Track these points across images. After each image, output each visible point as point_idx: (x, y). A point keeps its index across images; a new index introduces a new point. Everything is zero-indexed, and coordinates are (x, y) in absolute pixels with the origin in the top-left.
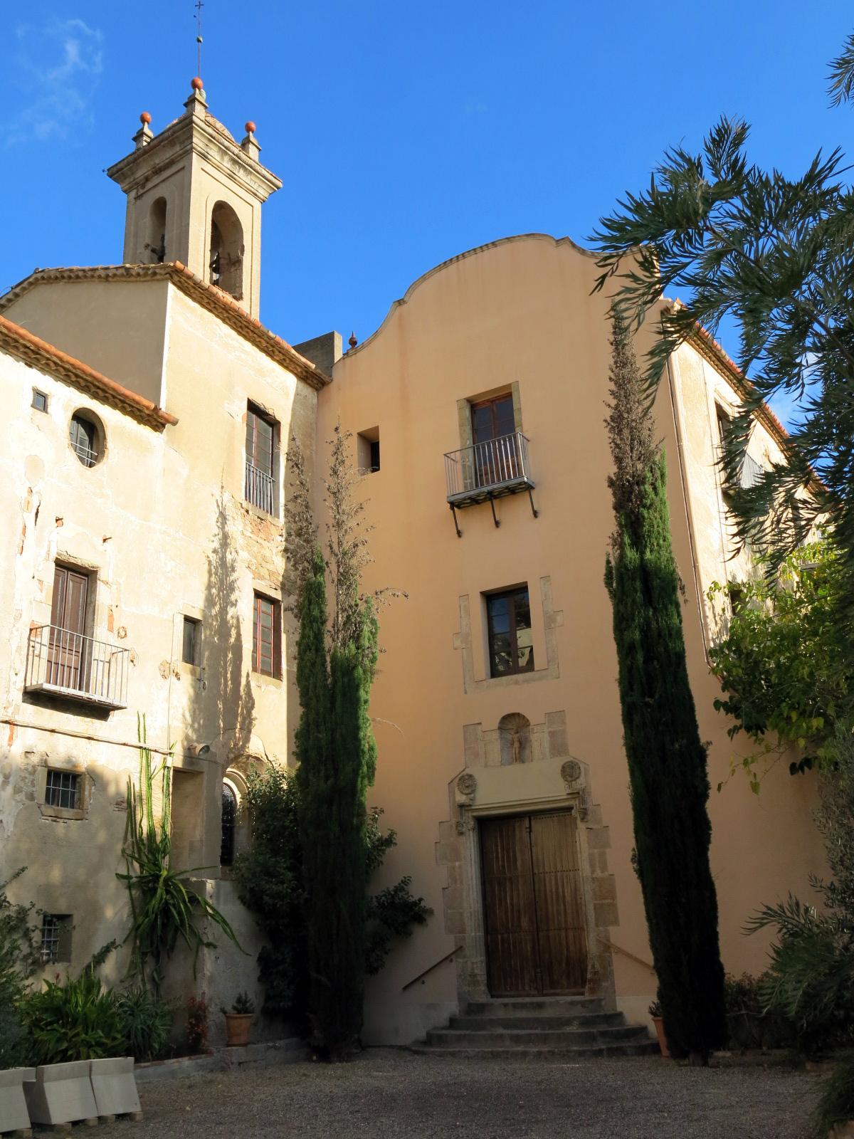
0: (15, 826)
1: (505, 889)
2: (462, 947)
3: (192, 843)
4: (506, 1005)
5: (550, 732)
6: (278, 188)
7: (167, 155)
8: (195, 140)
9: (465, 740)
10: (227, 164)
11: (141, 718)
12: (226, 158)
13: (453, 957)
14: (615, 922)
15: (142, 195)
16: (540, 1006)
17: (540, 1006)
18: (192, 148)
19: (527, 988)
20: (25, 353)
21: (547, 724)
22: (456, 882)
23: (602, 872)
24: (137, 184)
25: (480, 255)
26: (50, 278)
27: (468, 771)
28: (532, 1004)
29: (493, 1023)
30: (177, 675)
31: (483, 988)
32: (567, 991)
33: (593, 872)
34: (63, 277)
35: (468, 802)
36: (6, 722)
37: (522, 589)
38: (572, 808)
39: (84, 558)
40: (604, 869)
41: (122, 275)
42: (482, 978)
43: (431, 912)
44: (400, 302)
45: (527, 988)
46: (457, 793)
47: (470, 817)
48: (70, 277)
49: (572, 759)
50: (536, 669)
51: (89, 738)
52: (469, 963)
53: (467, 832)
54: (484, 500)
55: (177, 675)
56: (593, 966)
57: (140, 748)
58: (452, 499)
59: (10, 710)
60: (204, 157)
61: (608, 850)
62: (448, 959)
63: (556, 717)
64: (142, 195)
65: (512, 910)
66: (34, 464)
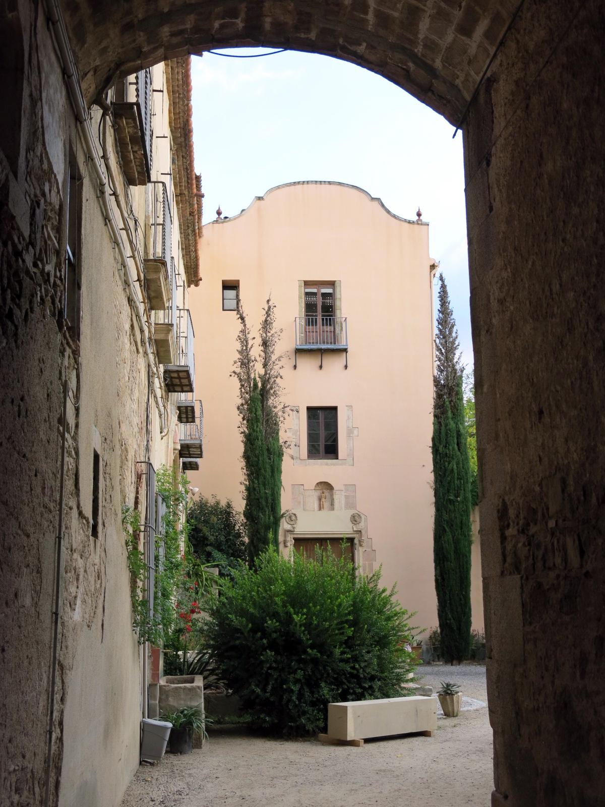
9: (293, 493)
25: (318, 185)
37: (335, 409)
44: (260, 198)
50: (339, 458)
61: (374, 563)
63: (351, 488)
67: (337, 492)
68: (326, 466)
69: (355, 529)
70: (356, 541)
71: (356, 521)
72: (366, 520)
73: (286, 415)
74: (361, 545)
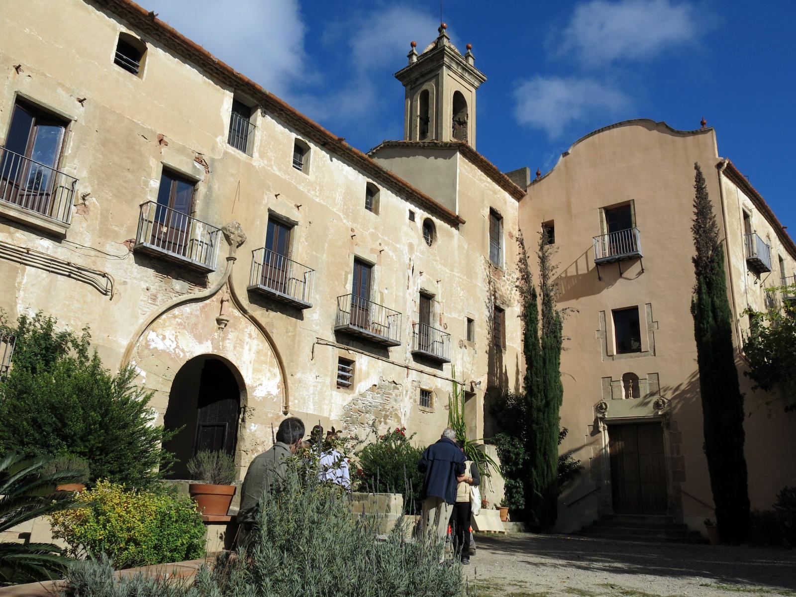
0: (410, 413)
3: (470, 427)
6: (484, 80)
7: (429, 67)
8: (445, 59)
10: (460, 70)
11: (453, 367)
12: (460, 67)
15: (414, 88)
18: (444, 63)
20: (407, 194)
24: (411, 81)
26: (392, 145)
30: (465, 346)
34: (399, 145)
36: (406, 367)
39: (430, 290)
41: (433, 146)
48: (403, 146)
51: (435, 376)
54: (614, 262)
55: (465, 346)
57: (453, 381)
58: (597, 261)
59: (407, 361)
60: (449, 67)
64: (414, 88)
66: (411, 246)
73: (565, 316)
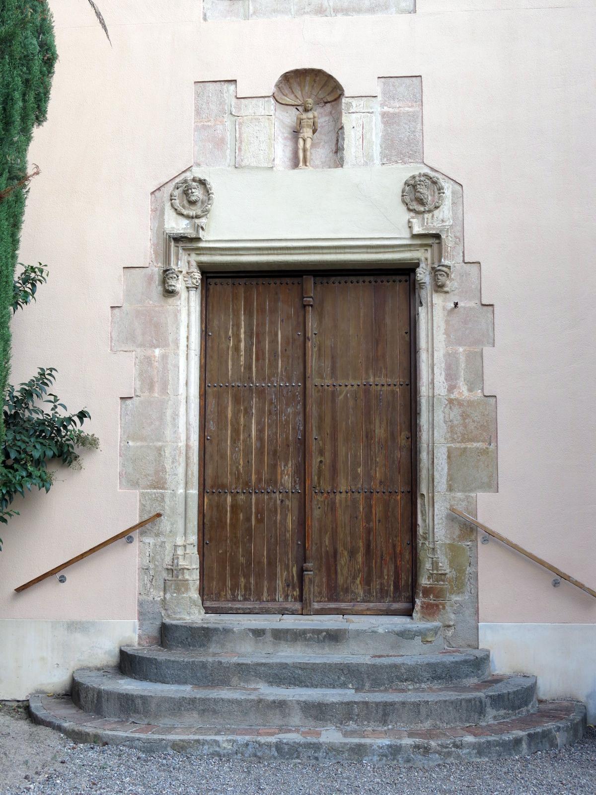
1: (247, 412)
2: (159, 515)
4: (258, 633)
5: (384, 115)
9: (198, 112)
13: (135, 534)
14: (492, 485)
16: (334, 637)
17: (334, 637)
19: (280, 597)
21: (379, 98)
22: (151, 388)
23: (470, 390)
27: (198, 173)
28: (318, 632)
29: (245, 671)
31: (195, 595)
32: (364, 606)
33: (451, 389)
35: (190, 233)
38: (417, 265)
40: (477, 378)
42: (193, 577)
43: (89, 443)
45: (280, 597)
46: (170, 214)
47: (194, 264)
49: (426, 171)
52: (169, 546)
53: (184, 294)
56: (435, 564)
61: (487, 351)
62: (125, 536)
65: (260, 451)
67: (354, 102)
68: (319, 19)
69: (417, 230)
70: (423, 275)
71: (421, 202)
72: (458, 199)
74: (439, 288)
